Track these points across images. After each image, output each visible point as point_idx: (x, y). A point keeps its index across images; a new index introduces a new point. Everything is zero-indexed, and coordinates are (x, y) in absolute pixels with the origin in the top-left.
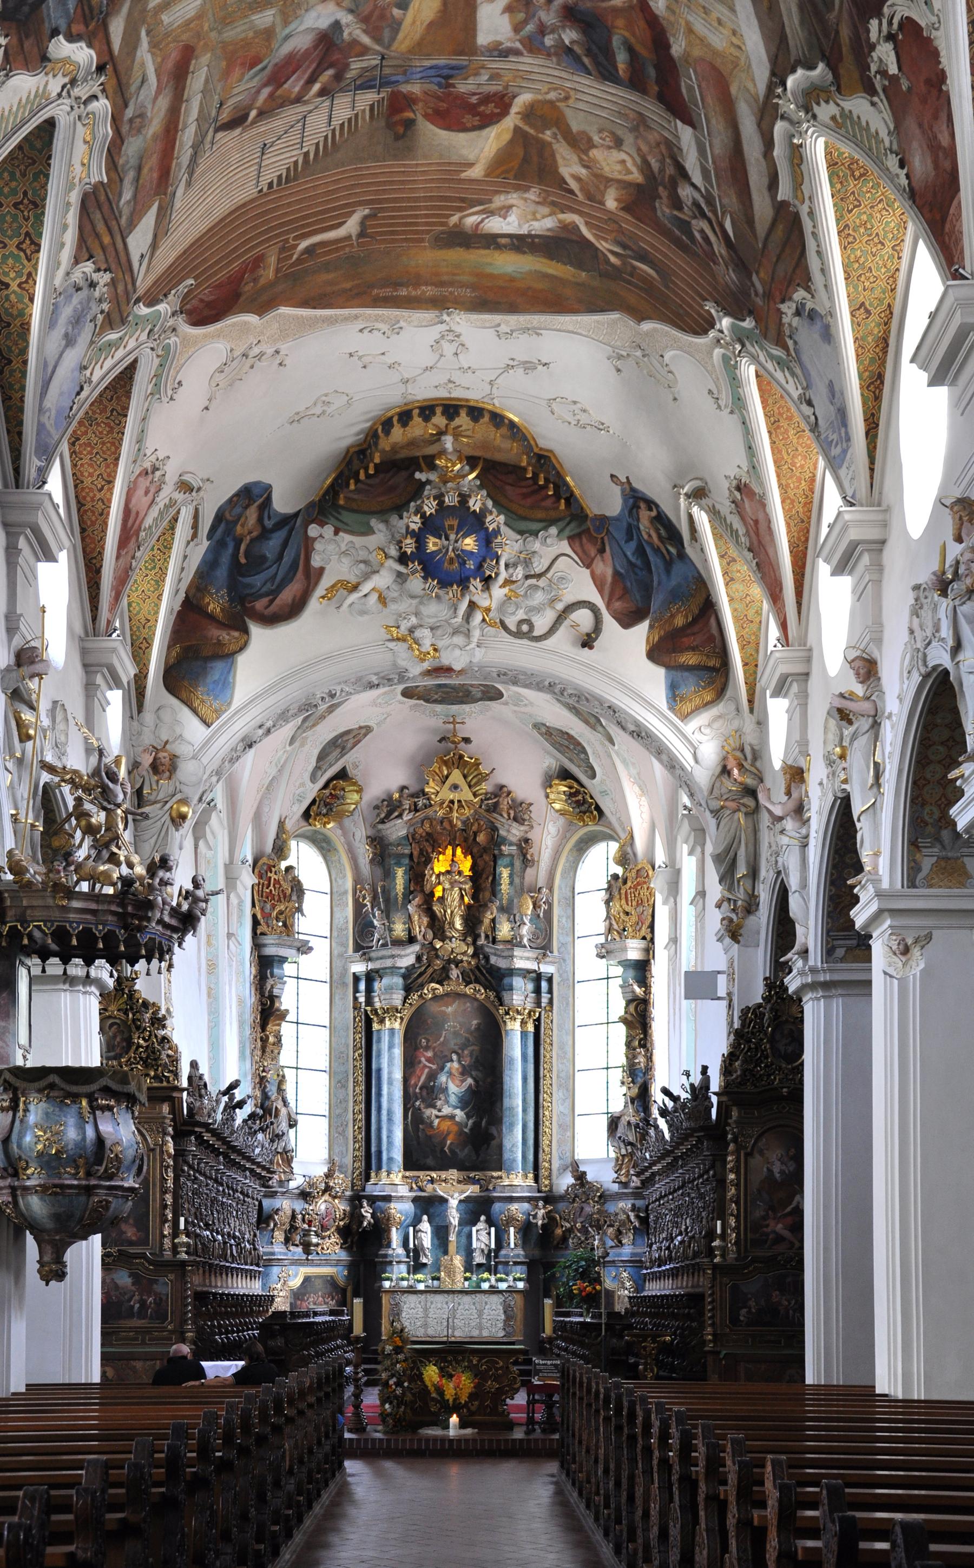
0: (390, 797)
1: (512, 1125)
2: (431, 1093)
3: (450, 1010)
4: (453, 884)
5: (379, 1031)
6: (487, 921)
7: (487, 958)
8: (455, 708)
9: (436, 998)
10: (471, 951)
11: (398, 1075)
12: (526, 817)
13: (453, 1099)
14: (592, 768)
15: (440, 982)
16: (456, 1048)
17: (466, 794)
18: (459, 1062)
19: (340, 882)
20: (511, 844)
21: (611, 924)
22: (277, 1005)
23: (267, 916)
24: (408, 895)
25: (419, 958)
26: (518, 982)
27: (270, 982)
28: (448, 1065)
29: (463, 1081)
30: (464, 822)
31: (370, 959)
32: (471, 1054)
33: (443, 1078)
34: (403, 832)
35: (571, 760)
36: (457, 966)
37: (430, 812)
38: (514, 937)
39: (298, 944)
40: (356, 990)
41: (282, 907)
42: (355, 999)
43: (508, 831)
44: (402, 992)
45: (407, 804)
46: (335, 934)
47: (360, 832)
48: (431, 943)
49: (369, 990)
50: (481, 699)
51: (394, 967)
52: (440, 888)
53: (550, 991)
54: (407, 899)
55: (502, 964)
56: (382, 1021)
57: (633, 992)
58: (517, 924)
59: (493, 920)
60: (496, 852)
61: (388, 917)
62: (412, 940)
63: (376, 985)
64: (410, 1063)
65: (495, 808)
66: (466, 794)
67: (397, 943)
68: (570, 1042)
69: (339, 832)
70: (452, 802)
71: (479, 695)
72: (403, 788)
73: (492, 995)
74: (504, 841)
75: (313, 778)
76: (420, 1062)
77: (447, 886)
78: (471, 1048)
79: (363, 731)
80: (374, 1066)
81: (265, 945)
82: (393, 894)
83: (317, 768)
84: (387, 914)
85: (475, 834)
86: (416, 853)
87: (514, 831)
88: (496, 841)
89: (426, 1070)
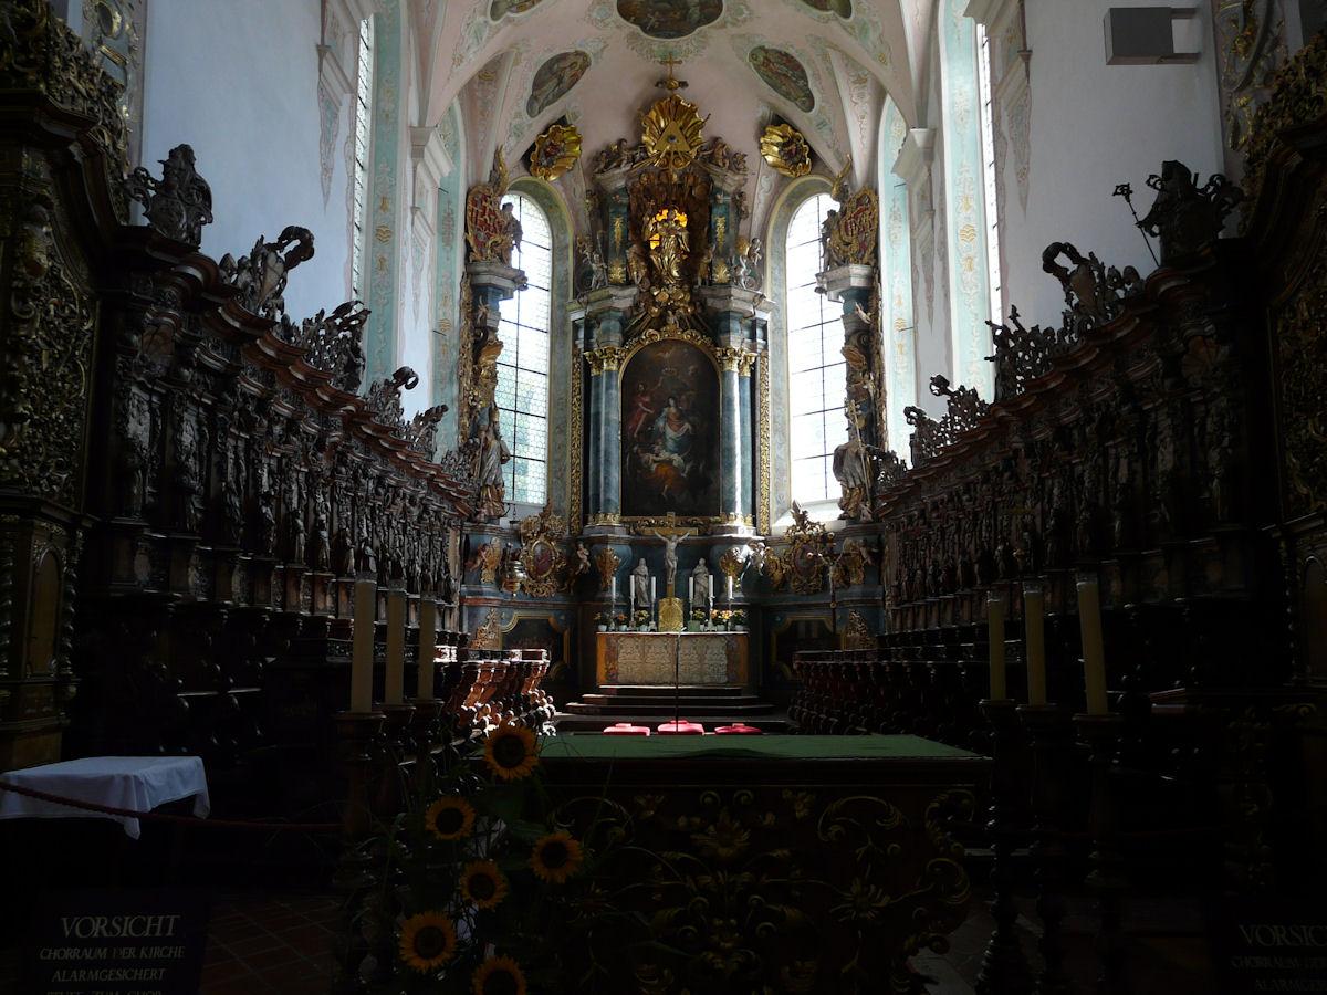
0: (608, 148)
1: (730, 466)
2: (649, 438)
3: (667, 355)
4: (669, 231)
5: (598, 377)
6: (703, 268)
7: (703, 305)
8: (671, 42)
9: (654, 344)
10: (688, 298)
11: (616, 416)
12: (741, 166)
13: (670, 444)
14: (810, 97)
15: (659, 330)
16: (674, 392)
17: (682, 146)
18: (676, 407)
19: (562, 237)
20: (726, 194)
21: (831, 256)
22: (490, 337)
23: (481, 245)
24: (626, 244)
25: (636, 306)
26: (735, 325)
27: (483, 309)
28: (666, 410)
29: (680, 426)
30: (680, 177)
31: (588, 303)
32: (688, 400)
33: (661, 424)
34: (621, 184)
35: (787, 95)
36: (674, 313)
37: (647, 163)
38: (731, 279)
39: (513, 274)
40: (576, 337)
41: (498, 239)
42: (575, 346)
43: (724, 181)
44: (620, 335)
45: (625, 155)
46: (556, 287)
47: (582, 186)
48: (649, 291)
49: (588, 337)
50: (700, 23)
51: (610, 308)
52: (656, 237)
53: (765, 338)
54: (626, 244)
55: (719, 305)
56: (600, 367)
57: (858, 316)
58: (733, 267)
59: (710, 265)
60: (712, 201)
61: (606, 263)
62: (629, 283)
63: (596, 333)
64: (628, 408)
65: (711, 158)
66: (682, 146)
67: (616, 284)
68: (785, 389)
69: (561, 188)
70: (668, 153)
71: (695, 13)
72: (620, 142)
73: (707, 340)
74: (720, 190)
75: (531, 111)
76: (638, 407)
77: (664, 233)
78: (688, 393)
79: (580, 61)
80: (592, 411)
81: (478, 274)
82: (611, 243)
83: (533, 98)
84: (605, 258)
85: (691, 187)
86: (633, 205)
87: (729, 181)
88: (711, 191)
89: (644, 415)
